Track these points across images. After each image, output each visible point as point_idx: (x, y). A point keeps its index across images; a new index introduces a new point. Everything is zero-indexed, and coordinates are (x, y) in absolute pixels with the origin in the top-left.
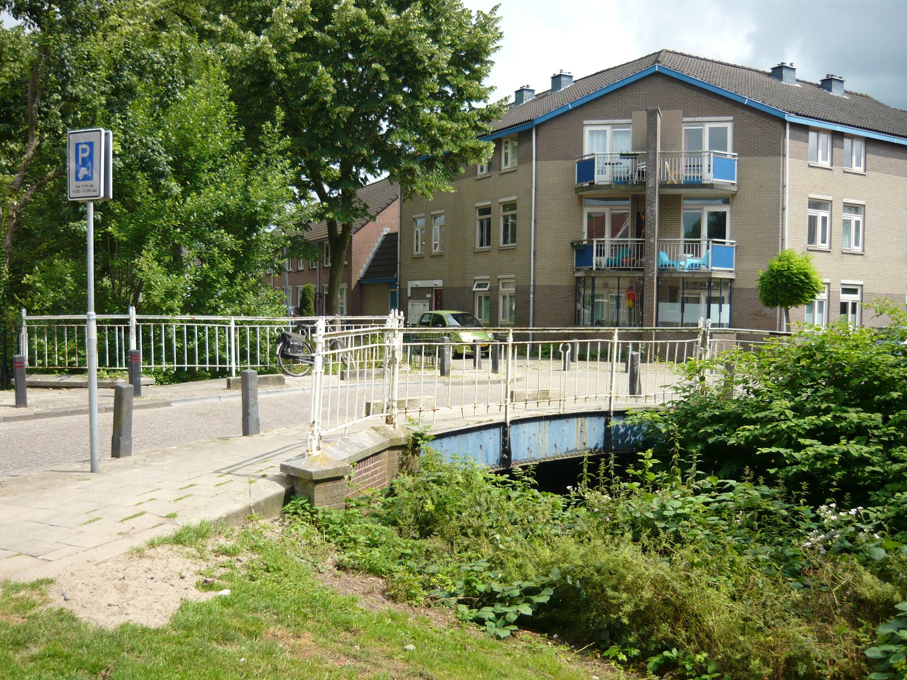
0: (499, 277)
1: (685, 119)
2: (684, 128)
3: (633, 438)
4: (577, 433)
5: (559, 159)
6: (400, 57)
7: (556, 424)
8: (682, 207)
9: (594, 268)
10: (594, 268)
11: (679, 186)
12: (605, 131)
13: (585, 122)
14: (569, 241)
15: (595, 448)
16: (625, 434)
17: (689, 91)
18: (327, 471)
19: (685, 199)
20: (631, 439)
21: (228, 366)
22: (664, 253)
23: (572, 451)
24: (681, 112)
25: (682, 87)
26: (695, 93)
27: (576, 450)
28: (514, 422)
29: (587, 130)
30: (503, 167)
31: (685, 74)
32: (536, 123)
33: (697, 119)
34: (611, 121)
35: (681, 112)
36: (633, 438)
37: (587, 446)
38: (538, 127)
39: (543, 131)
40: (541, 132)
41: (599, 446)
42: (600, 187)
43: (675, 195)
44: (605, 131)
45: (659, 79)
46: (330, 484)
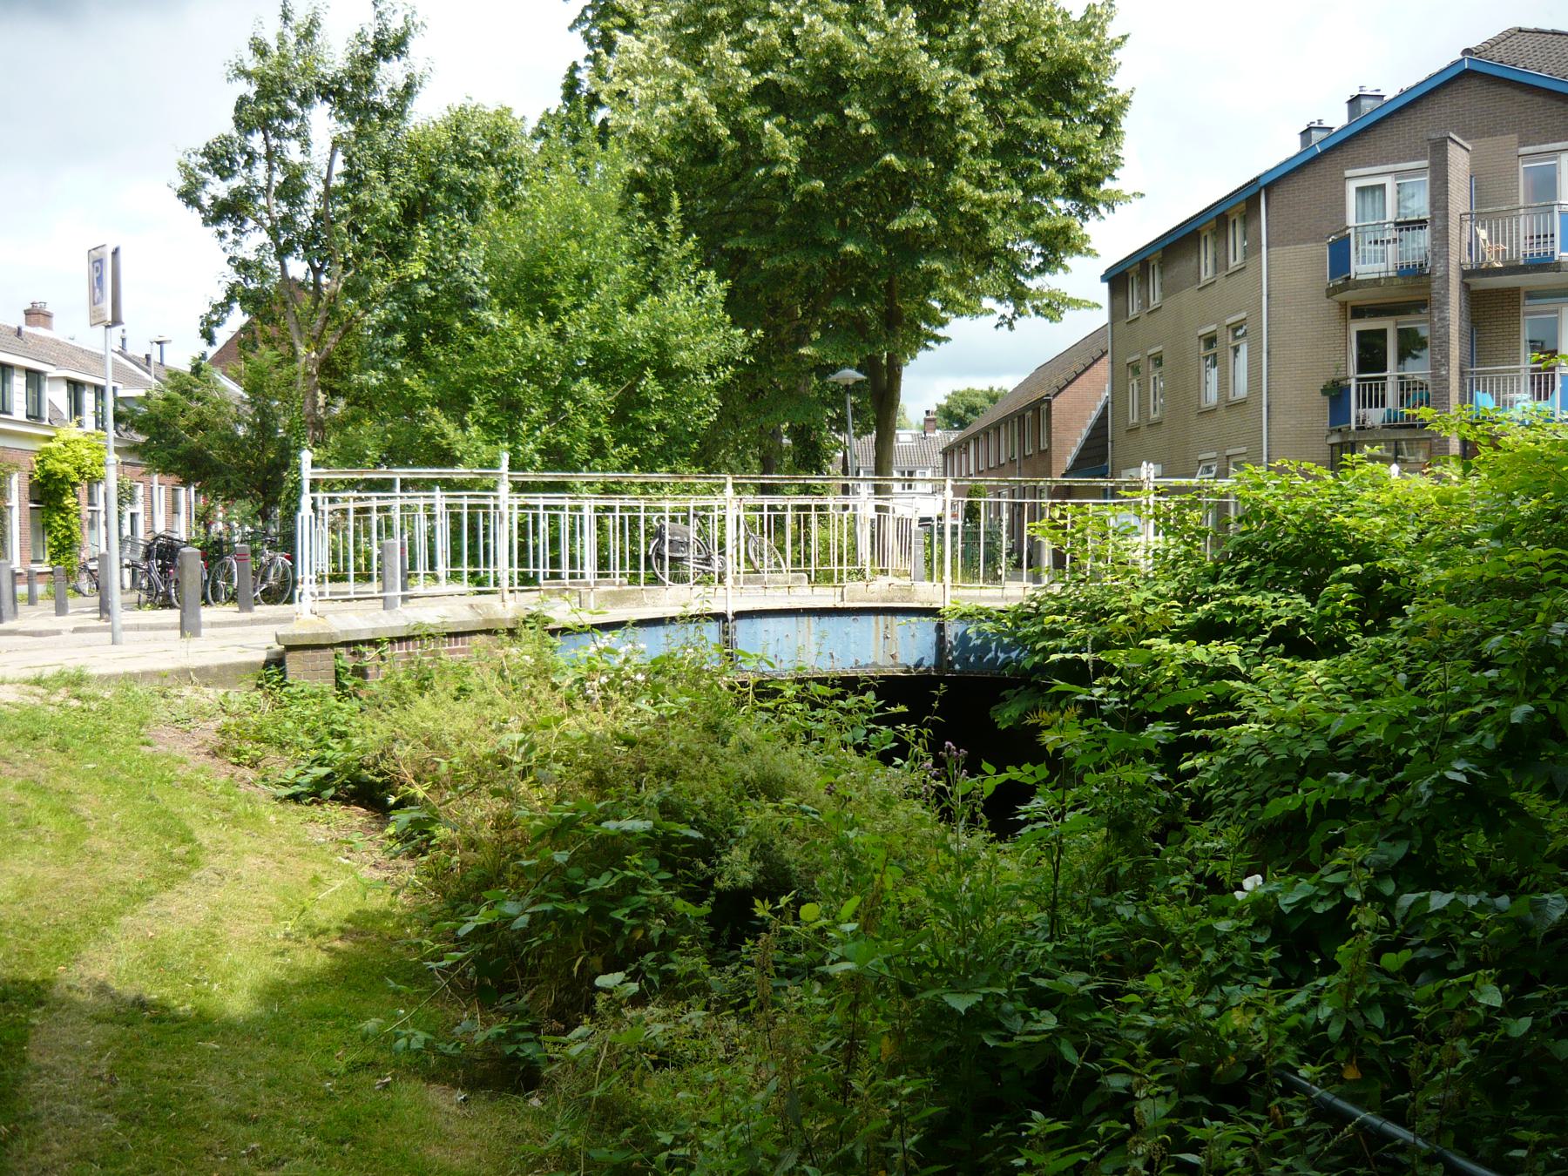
0: (1229, 452)
1: (1523, 150)
2: (1522, 167)
3: (1002, 656)
4: (877, 638)
5: (1304, 241)
6: (894, 95)
7: (835, 621)
8: (1523, 309)
9: (1353, 427)
10: (1353, 427)
11: (1511, 269)
12: (1382, 187)
13: (1348, 173)
14: (1322, 382)
15: (917, 666)
16: (985, 648)
17: (1528, 97)
18: (302, 636)
19: (1531, 295)
20: (997, 658)
21: (531, 569)
22: (1488, 395)
23: (867, 666)
24: (1515, 137)
25: (1516, 93)
26: (1540, 100)
27: (875, 664)
28: (740, 615)
29: (1351, 187)
30: (1231, 263)
31: (1520, 67)
32: (1263, 182)
33: (1545, 147)
34: (1391, 167)
35: (1515, 137)
36: (1002, 656)
37: (899, 661)
38: (1269, 188)
39: (1277, 194)
40: (1273, 197)
41: (926, 663)
42: (1360, 284)
43: (1509, 289)
44: (1382, 187)
45: (1475, 82)
46: (310, 653)
